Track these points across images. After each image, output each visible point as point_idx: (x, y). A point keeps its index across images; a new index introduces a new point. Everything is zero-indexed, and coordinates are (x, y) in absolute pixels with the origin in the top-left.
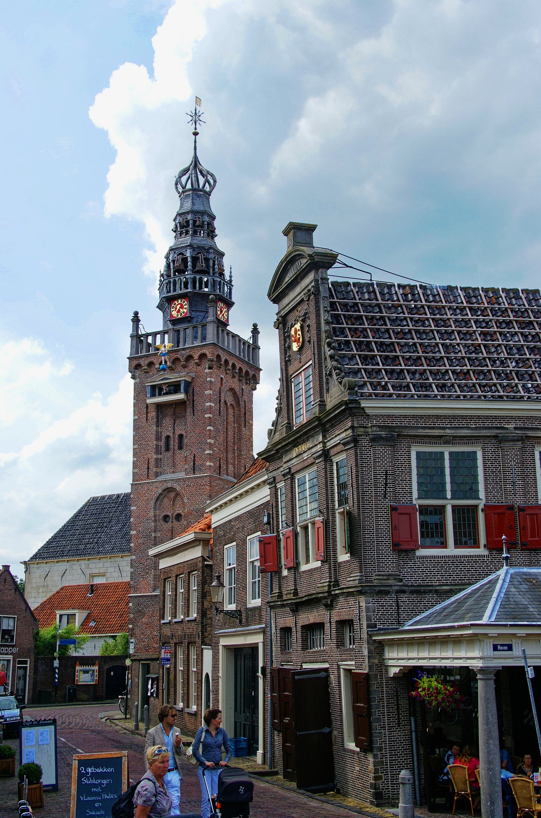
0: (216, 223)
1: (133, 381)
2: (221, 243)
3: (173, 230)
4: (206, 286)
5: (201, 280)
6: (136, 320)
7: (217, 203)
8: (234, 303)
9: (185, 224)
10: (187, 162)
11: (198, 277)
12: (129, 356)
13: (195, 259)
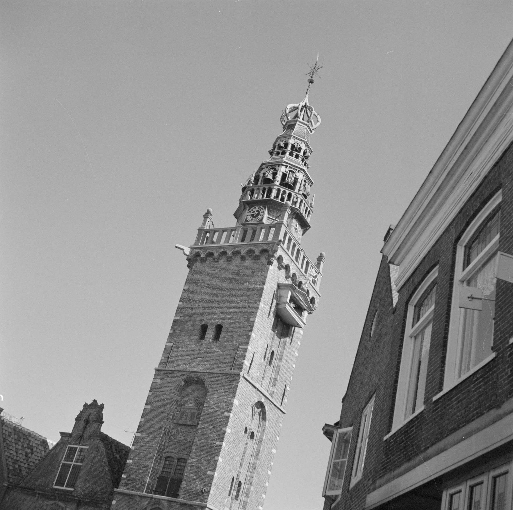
5: (284, 192)
6: (207, 214)
9: (283, 146)
13: (284, 176)
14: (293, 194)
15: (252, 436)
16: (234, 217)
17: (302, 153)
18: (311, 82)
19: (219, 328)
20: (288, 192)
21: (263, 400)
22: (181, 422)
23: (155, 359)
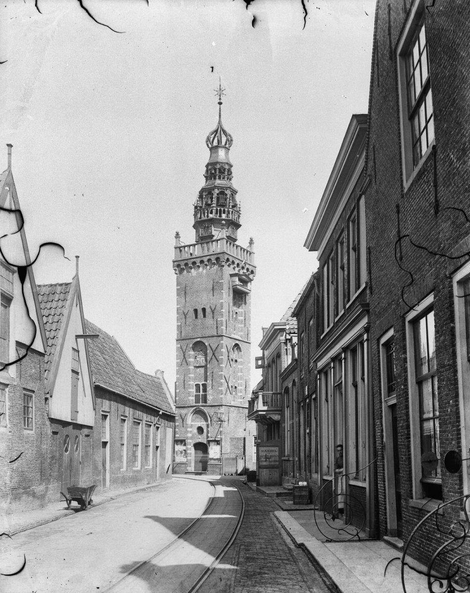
0: (233, 169)
1: (176, 275)
2: (235, 183)
3: (204, 175)
4: (224, 213)
5: (220, 210)
6: (177, 235)
7: (234, 156)
8: (241, 225)
10: (214, 127)
11: (219, 209)
12: (173, 258)
14: (226, 209)
15: (236, 361)
16: (193, 228)
17: (226, 173)
18: (220, 103)
19: (204, 310)
20: (222, 209)
21: (237, 342)
22: (197, 365)
23: (174, 334)
